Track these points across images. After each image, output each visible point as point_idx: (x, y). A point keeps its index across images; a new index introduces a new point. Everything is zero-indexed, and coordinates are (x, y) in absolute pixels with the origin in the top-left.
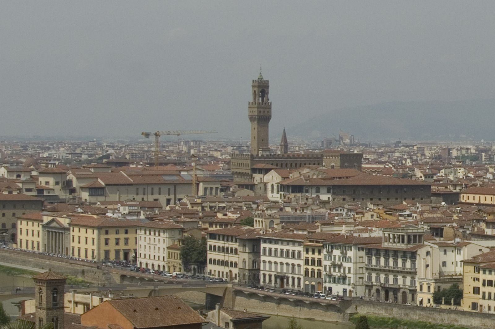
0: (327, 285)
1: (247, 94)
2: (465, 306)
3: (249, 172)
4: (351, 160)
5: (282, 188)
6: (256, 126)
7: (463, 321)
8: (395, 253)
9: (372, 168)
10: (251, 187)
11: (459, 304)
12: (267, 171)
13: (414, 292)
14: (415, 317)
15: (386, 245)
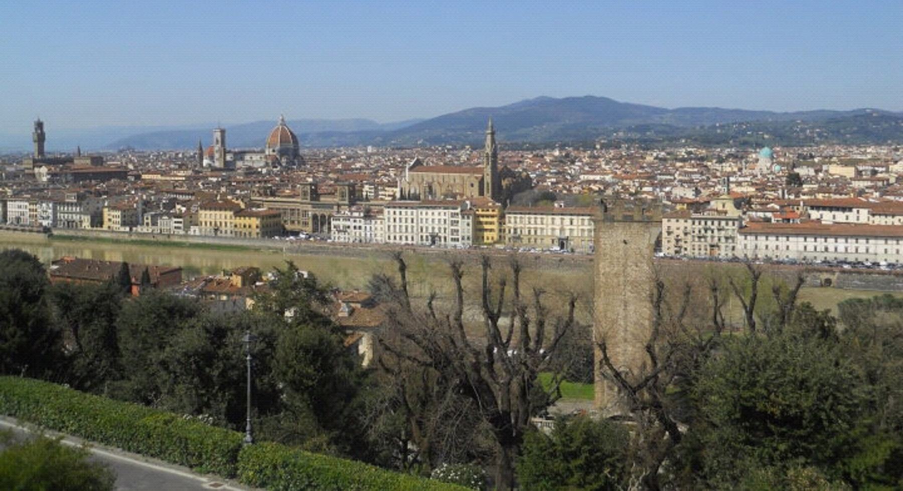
0: (40, 221)
1: (31, 130)
2: (105, 228)
3: (31, 166)
4: (97, 160)
5: (48, 174)
6: (36, 144)
7: (102, 235)
8: (72, 204)
9: (113, 164)
10: (33, 175)
11: (101, 226)
12: (40, 167)
13: (81, 222)
14: (80, 234)
15: (67, 200)
